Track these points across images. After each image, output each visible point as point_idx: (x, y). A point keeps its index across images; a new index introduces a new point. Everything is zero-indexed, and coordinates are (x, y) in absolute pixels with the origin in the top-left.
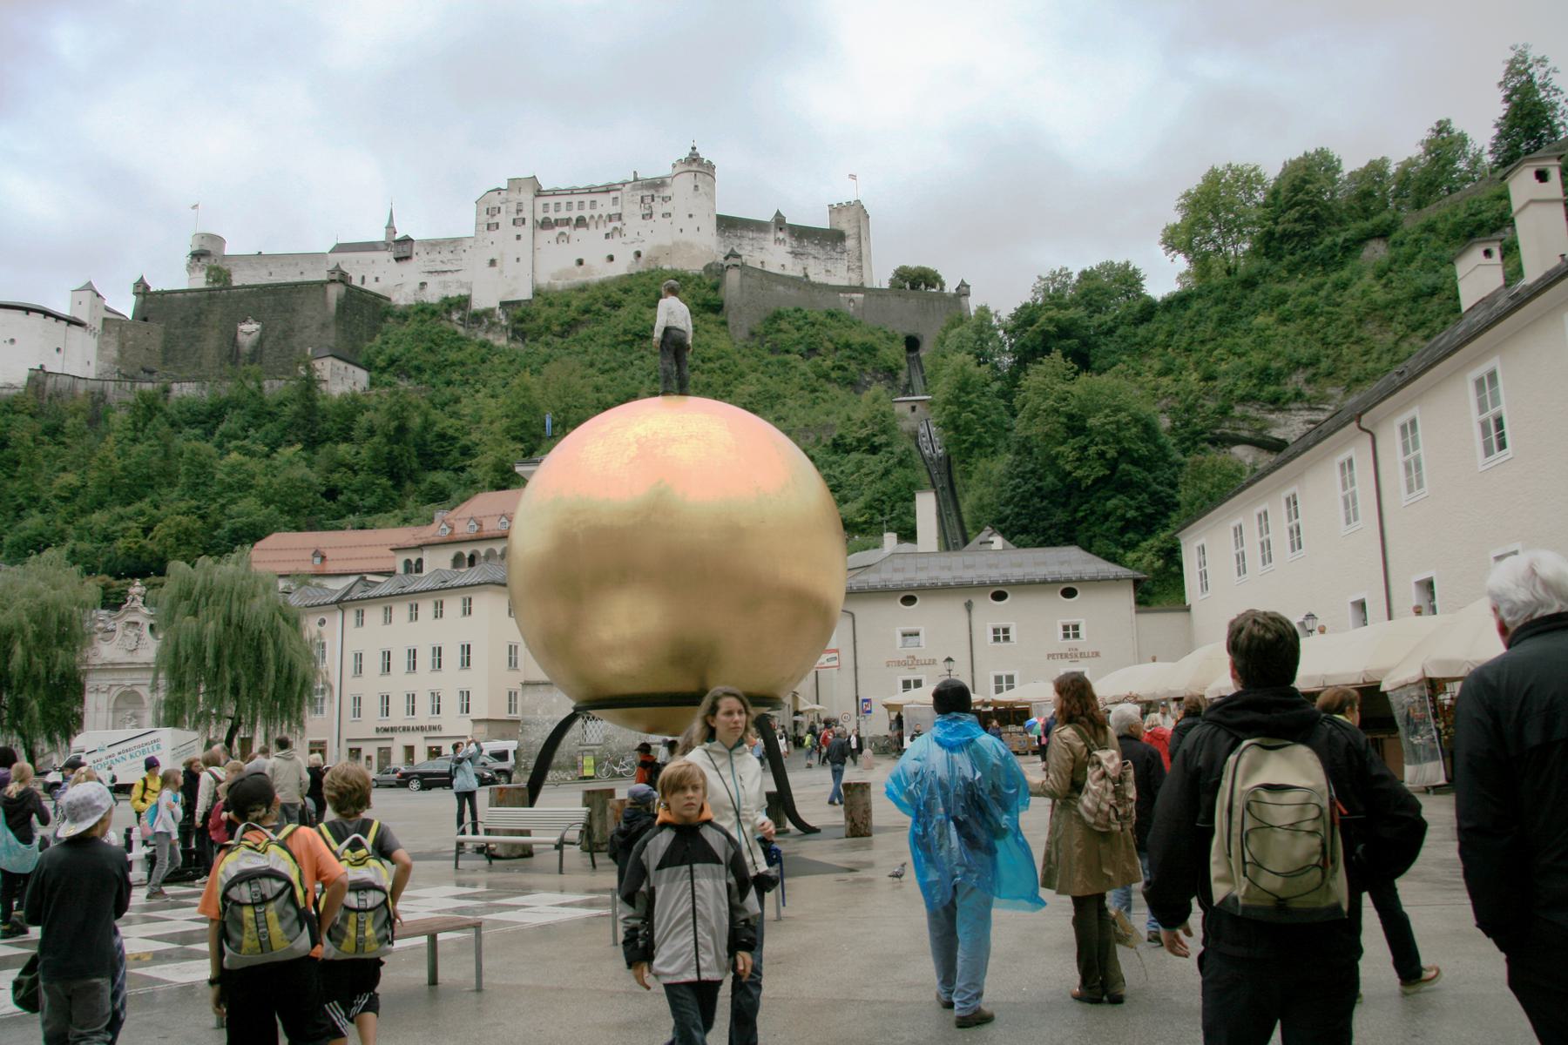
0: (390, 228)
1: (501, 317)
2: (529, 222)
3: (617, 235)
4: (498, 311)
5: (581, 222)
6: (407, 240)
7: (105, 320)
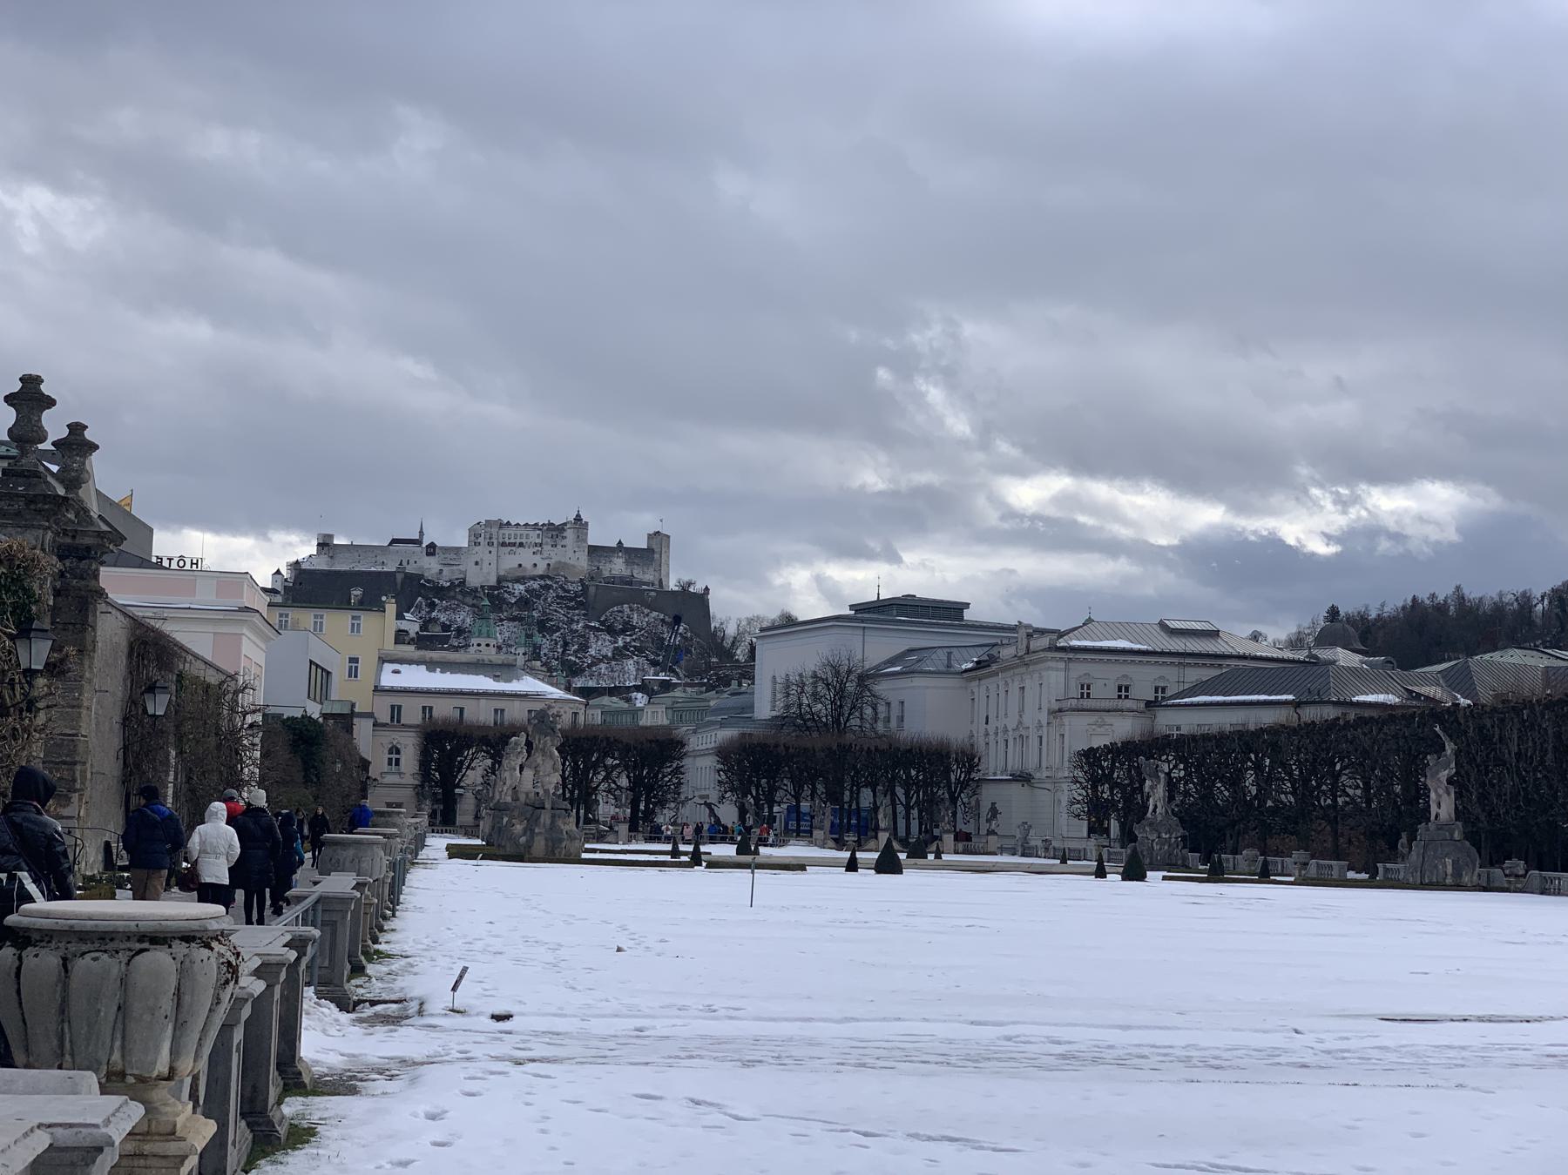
0: (421, 533)
3: (539, 553)
5: (521, 545)
6: (432, 546)
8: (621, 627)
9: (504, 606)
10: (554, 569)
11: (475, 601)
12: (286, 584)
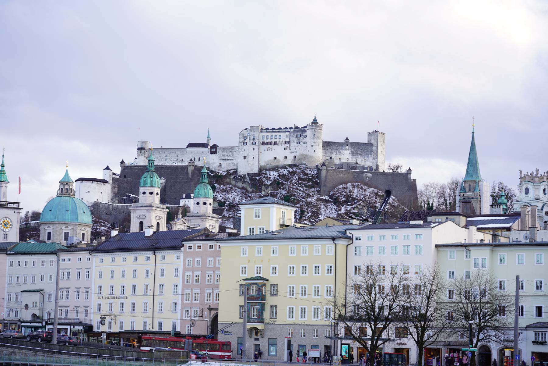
0: (208, 138)
1: (248, 179)
2: (257, 144)
4: (246, 176)
5: (276, 143)
7: (113, 178)
8: (344, 199)
9: (263, 187)
10: (299, 160)
11: (244, 185)
12: (114, 176)
